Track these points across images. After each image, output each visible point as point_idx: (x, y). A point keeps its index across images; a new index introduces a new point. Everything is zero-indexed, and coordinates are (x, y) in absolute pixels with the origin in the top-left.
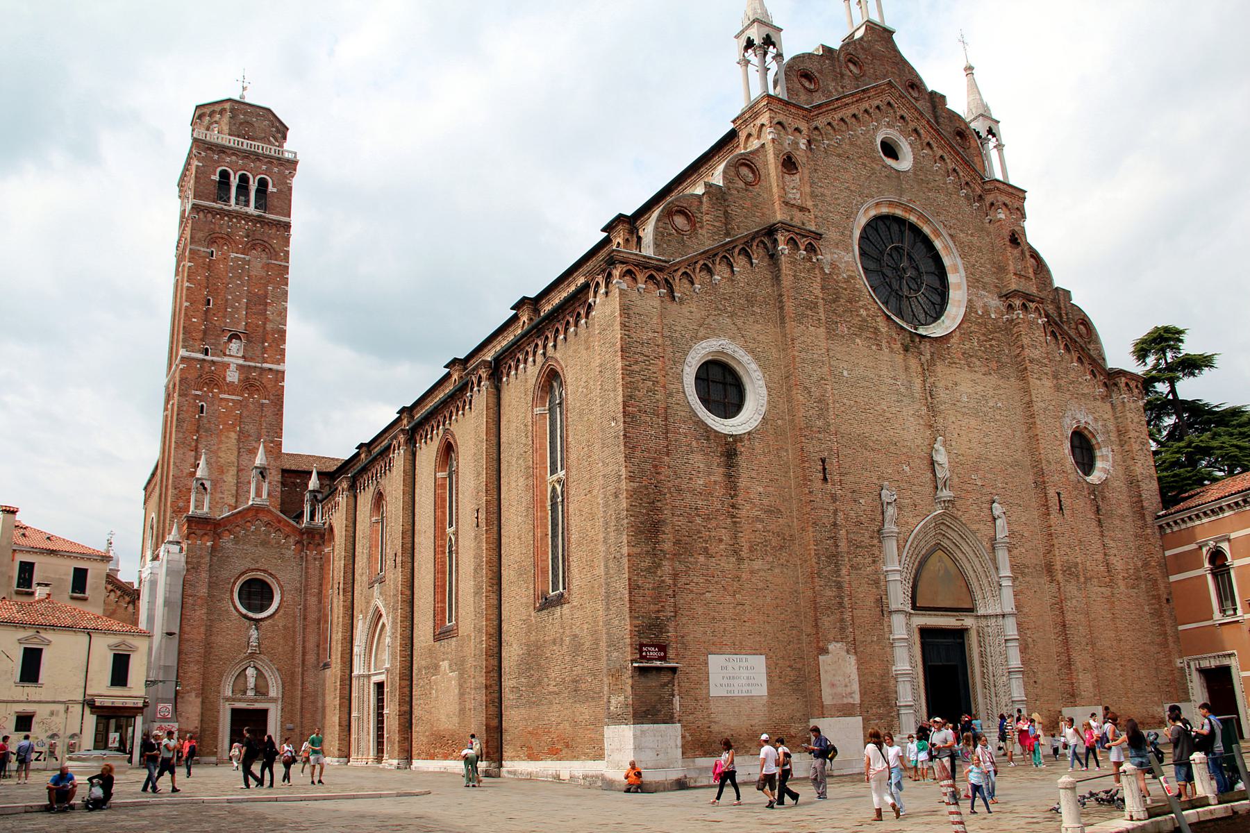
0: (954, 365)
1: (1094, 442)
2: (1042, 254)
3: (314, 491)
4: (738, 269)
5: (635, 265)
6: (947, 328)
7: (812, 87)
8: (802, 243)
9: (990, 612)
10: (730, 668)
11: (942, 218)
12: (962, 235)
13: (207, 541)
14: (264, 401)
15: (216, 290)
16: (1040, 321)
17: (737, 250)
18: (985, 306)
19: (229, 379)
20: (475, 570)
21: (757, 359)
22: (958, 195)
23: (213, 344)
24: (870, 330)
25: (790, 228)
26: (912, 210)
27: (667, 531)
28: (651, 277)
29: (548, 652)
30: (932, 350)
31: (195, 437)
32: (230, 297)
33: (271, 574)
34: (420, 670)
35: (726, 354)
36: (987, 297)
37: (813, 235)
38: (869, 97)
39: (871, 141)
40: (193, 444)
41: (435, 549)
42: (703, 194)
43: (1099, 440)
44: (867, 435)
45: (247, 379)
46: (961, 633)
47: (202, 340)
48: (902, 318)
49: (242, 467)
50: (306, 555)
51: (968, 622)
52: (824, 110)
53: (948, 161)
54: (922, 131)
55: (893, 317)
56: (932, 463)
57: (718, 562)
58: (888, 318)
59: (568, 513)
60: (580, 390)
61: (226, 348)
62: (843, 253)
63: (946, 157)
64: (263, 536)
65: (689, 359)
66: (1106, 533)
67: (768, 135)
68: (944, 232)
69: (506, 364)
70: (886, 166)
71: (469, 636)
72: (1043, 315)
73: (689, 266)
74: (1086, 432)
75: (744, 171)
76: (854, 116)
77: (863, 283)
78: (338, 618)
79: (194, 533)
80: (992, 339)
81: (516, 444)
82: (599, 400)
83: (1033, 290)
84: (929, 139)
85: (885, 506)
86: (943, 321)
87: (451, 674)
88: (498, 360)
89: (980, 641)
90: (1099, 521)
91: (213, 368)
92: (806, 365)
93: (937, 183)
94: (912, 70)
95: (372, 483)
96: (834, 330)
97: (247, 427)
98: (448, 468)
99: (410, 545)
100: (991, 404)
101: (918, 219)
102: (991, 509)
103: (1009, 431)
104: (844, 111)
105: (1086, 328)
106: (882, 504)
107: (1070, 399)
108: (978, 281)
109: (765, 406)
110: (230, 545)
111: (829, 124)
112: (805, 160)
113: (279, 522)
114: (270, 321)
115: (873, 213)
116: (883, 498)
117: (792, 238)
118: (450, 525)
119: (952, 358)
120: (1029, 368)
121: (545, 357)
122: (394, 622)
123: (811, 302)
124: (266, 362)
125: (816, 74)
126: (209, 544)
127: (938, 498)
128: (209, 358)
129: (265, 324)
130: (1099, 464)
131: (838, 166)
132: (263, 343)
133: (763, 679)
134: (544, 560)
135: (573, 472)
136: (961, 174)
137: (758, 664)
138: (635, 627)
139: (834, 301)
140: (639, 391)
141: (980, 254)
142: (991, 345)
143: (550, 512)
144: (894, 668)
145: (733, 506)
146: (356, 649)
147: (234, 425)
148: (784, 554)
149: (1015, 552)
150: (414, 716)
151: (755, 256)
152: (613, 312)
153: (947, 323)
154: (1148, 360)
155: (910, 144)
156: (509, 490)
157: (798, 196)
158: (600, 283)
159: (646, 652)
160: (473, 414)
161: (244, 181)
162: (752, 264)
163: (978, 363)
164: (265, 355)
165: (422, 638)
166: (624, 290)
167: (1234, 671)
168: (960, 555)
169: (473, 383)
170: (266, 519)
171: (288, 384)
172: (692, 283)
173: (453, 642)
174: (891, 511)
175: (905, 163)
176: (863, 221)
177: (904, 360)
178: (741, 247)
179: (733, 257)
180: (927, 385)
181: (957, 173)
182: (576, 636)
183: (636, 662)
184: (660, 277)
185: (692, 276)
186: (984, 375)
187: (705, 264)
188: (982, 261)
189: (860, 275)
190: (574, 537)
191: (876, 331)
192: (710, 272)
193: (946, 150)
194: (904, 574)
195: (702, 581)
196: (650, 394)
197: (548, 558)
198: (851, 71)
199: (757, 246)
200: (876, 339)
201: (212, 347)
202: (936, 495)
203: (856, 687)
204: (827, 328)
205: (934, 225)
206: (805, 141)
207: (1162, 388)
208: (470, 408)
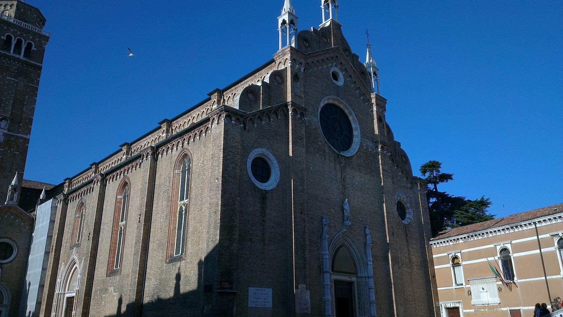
0: (353, 169)
1: (406, 206)
2: (390, 127)
4: (272, 120)
5: (231, 113)
6: (352, 153)
7: (307, 45)
8: (299, 111)
9: (363, 275)
10: (257, 294)
14: (16, 153)
16: (388, 154)
17: (272, 112)
18: (367, 146)
20: (136, 243)
21: (277, 159)
22: (360, 99)
25: (295, 105)
26: (341, 103)
27: (236, 230)
28: (238, 119)
29: (171, 283)
33: (13, 240)
34: (96, 291)
35: (265, 155)
36: (368, 142)
37: (304, 109)
38: (329, 53)
39: (328, 72)
41: (112, 232)
42: (261, 86)
43: (408, 206)
44: (318, 195)
46: (351, 284)
48: (334, 147)
51: (354, 279)
52: (311, 56)
54: (348, 70)
55: (331, 147)
56: (343, 209)
57: (256, 245)
59: (188, 218)
60: (200, 164)
63: (357, 82)
65: (250, 156)
66: (409, 245)
67: (288, 64)
68: (354, 114)
69: (162, 149)
70: (333, 83)
71: (128, 276)
72: (389, 152)
73: (253, 116)
74: (403, 202)
75: (278, 78)
76: (323, 60)
77: (320, 131)
78: (50, 264)
80: (369, 160)
81: (163, 186)
82: (210, 170)
83: (387, 141)
85: (324, 226)
87: (114, 294)
88: (159, 146)
89: (358, 288)
90: (407, 240)
92: (297, 163)
94: (347, 43)
95: (78, 198)
98: (123, 194)
100: (367, 186)
101: (344, 107)
102: (365, 231)
103: (373, 199)
105: (405, 159)
106: (323, 225)
107: (398, 187)
109: (279, 179)
112: (302, 76)
113: (21, 214)
115: (326, 102)
116: (323, 222)
117: (295, 109)
118: (122, 221)
121: (182, 148)
122: (85, 266)
125: (309, 40)
127: (344, 224)
130: (407, 216)
132: (20, 124)
133: (270, 300)
134: (173, 240)
135: (193, 201)
136: (362, 90)
137: (269, 292)
138: (220, 273)
140: (229, 168)
142: (368, 162)
143: (178, 218)
144: (324, 297)
145: (263, 221)
146: (58, 280)
148: (282, 243)
149: (374, 250)
150: (89, 315)
151: (279, 115)
152: (220, 132)
153: (352, 151)
154: (426, 174)
155: (343, 75)
156: (157, 207)
157: (298, 91)
158: (215, 119)
159: (223, 285)
160: (142, 170)
161: (19, 43)
162: (278, 118)
163: (362, 169)
164: (20, 130)
165: (100, 275)
166: (226, 123)
167: (461, 310)
168: (352, 249)
169: (144, 155)
171: (30, 145)
172: (253, 123)
173: (118, 278)
174: (326, 228)
175: (340, 82)
176: (322, 105)
177: (335, 165)
178: (274, 110)
179: (270, 114)
180: (343, 176)
181: (361, 90)
182: (187, 276)
183: (218, 289)
184: (241, 119)
185: (254, 120)
186: (365, 174)
187: (259, 116)
189: (319, 128)
190: (190, 229)
191: (325, 151)
192: (261, 120)
194: (329, 256)
195: (248, 253)
196: (234, 169)
197: (175, 239)
198: (323, 40)
199: (281, 110)
200: (324, 155)
202: (343, 222)
203: (309, 306)
204: (306, 149)
206: (303, 68)
207: (431, 186)
208: (140, 167)
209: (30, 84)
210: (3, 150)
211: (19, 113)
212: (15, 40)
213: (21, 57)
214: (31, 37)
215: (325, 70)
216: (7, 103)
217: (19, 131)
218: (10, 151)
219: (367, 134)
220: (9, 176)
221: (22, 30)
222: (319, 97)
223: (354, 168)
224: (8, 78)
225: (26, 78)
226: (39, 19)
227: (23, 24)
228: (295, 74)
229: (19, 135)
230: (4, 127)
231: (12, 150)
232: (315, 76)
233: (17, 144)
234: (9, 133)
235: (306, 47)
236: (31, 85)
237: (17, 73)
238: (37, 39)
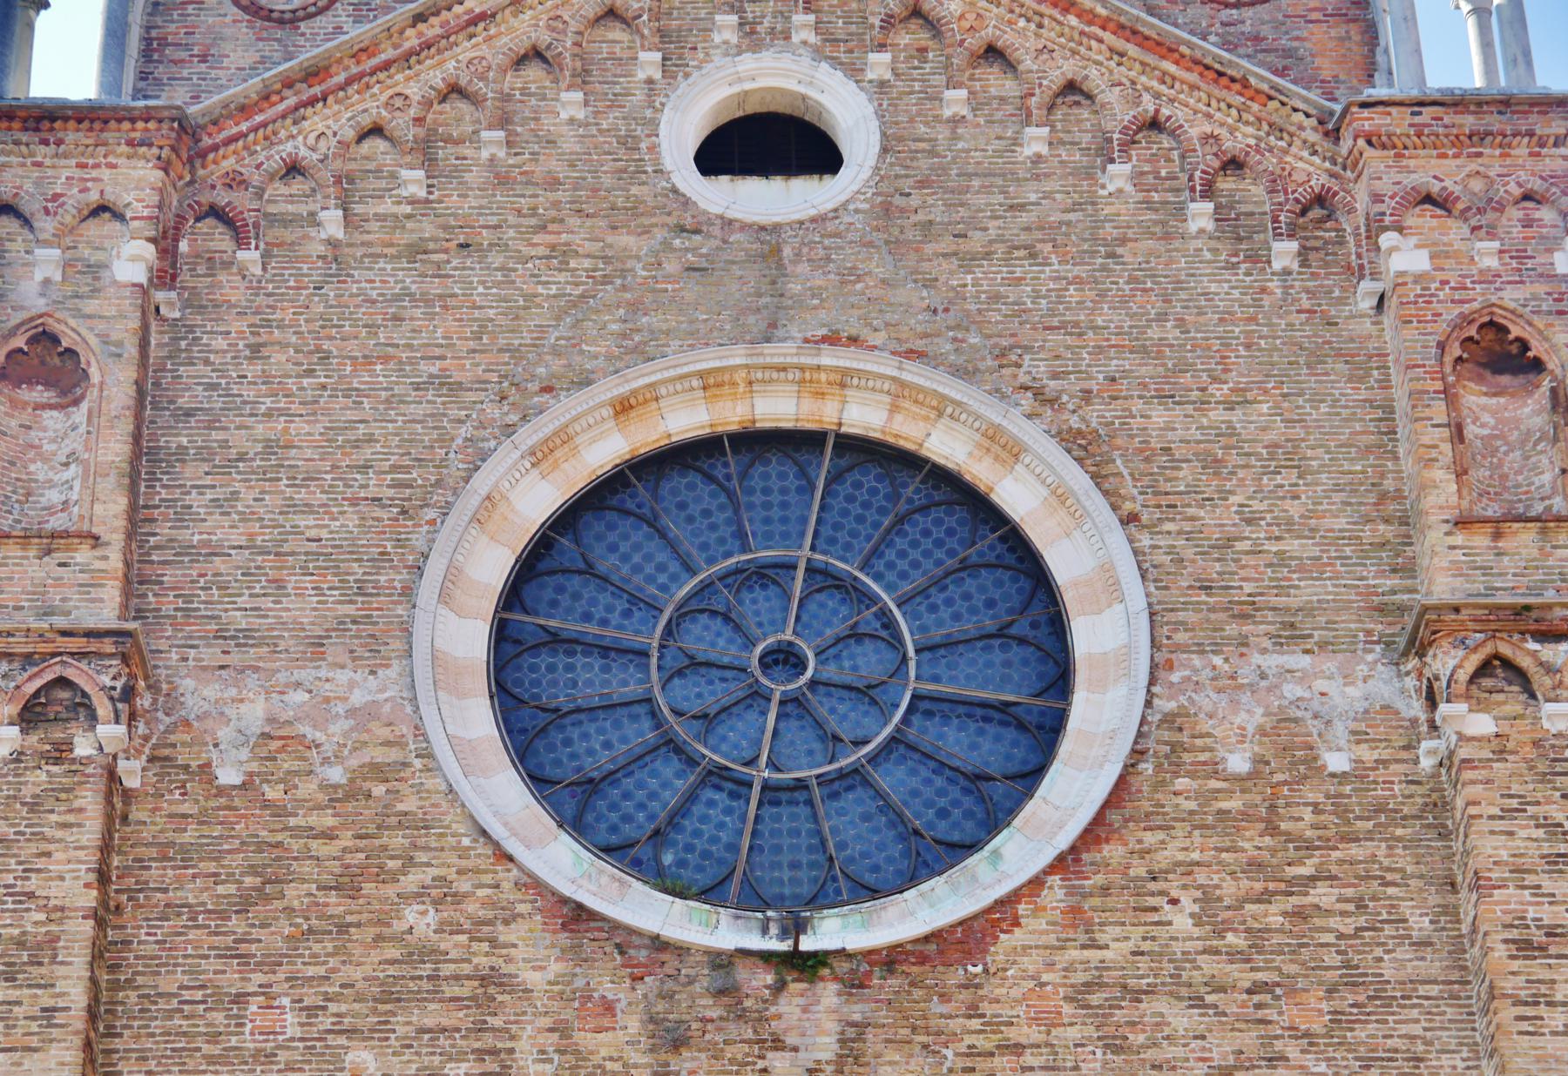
11: (1036, 367)
12: (1159, 416)
24: (457, 991)
30: (857, 1012)
36: (1304, 678)
37: (74, 644)
52: (340, 78)
53: (1111, 96)
58: (576, 917)
62: (343, 676)
63: (1095, 79)
68: (1033, 435)
76: (536, 54)
80: (1313, 879)
84: (988, 33)
86: (996, 853)
93: (1024, 218)
96: (214, 1038)
101: (894, 409)
104: (465, 50)
108: (1245, 612)
111: (376, 130)
119: (994, 1026)
120: (1508, 985)
123: (21, 944)
131: (397, 298)
139: (244, 905)
141: (1287, 478)
142: (1299, 914)
163: (1181, 1019)
188: (1294, 509)
189: (427, 754)
193: (1098, 52)
200: (480, 1028)
205: (978, 417)
215: (569, 144)
219: (1282, 590)
222: (445, 440)
223: (1017, 1049)
228: (20, 342)
232: (416, 251)
235: (281, 22)
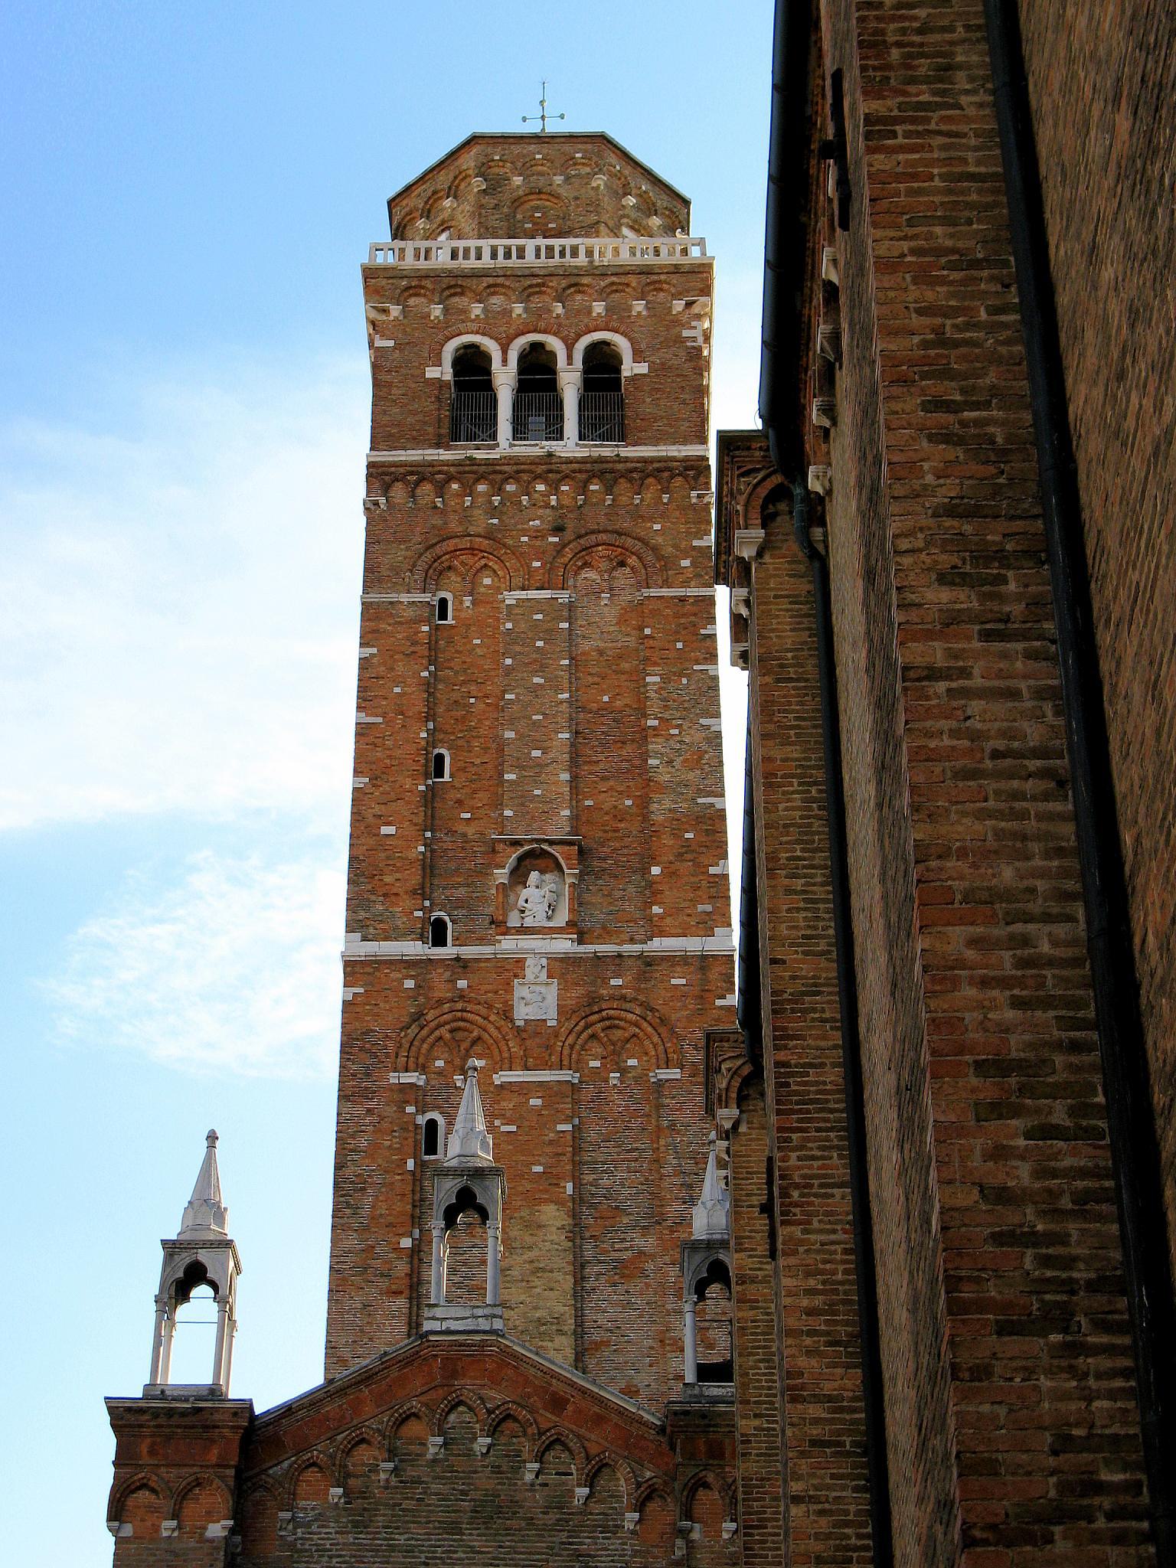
3: (709, 1245)
13: (210, 1516)
14: (664, 1074)
15: (462, 720)
19: (522, 1013)
23: (459, 904)
31: (406, 1243)
32: (510, 735)
40: (402, 1268)
45: (593, 999)
47: (422, 892)
49: (596, 1338)
50: (690, 1545)
61: (506, 908)
64: (485, 1482)
79: (144, 1486)
91: (462, 984)
97: (605, 1182)
99: (833, 1076)
110: (328, 1534)
114: (662, 789)
124: (662, 934)
126: (217, 1530)
128: (448, 951)
129: (644, 803)
147: (551, 1178)
164: (656, 910)
170: (496, 1396)
201: (460, 913)
209: (654, 592)
210: (565, 1075)
211: (629, 803)
212: (505, 362)
213: (570, 445)
214: (599, 308)
216: (536, 753)
217: (649, 919)
218: (624, 1071)
220: (652, 1256)
221: (531, 283)
224: (511, 598)
225: (622, 564)
226: (631, 200)
227: (532, 251)
229: (659, 945)
230: (549, 918)
231: (632, 1062)
233: (652, 1010)
234: (582, 949)
236: (665, 592)
237: (560, 549)
238: (639, 306)
